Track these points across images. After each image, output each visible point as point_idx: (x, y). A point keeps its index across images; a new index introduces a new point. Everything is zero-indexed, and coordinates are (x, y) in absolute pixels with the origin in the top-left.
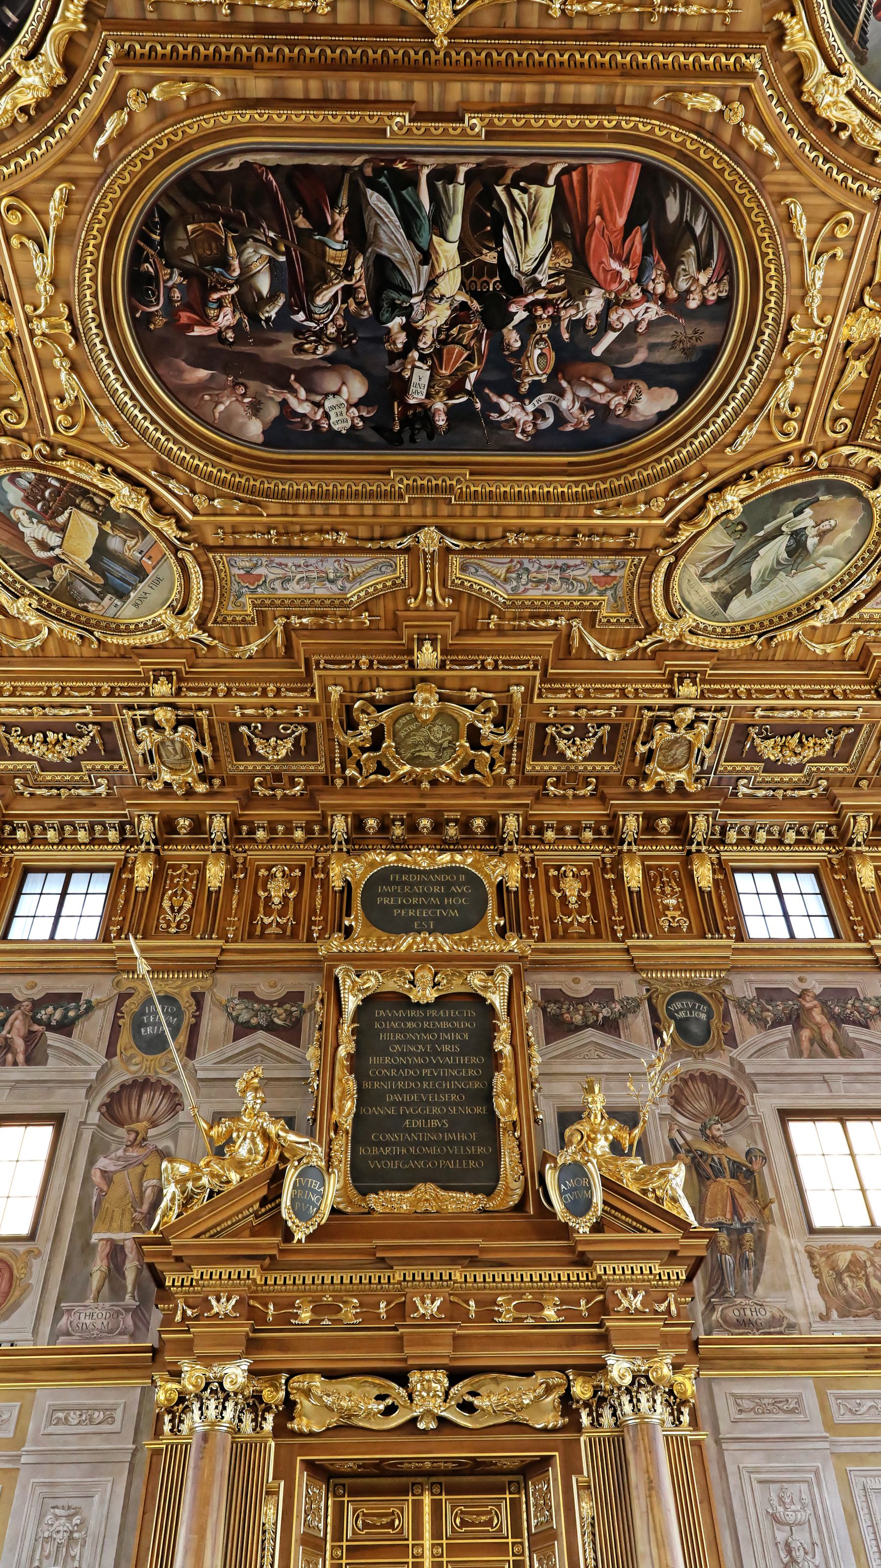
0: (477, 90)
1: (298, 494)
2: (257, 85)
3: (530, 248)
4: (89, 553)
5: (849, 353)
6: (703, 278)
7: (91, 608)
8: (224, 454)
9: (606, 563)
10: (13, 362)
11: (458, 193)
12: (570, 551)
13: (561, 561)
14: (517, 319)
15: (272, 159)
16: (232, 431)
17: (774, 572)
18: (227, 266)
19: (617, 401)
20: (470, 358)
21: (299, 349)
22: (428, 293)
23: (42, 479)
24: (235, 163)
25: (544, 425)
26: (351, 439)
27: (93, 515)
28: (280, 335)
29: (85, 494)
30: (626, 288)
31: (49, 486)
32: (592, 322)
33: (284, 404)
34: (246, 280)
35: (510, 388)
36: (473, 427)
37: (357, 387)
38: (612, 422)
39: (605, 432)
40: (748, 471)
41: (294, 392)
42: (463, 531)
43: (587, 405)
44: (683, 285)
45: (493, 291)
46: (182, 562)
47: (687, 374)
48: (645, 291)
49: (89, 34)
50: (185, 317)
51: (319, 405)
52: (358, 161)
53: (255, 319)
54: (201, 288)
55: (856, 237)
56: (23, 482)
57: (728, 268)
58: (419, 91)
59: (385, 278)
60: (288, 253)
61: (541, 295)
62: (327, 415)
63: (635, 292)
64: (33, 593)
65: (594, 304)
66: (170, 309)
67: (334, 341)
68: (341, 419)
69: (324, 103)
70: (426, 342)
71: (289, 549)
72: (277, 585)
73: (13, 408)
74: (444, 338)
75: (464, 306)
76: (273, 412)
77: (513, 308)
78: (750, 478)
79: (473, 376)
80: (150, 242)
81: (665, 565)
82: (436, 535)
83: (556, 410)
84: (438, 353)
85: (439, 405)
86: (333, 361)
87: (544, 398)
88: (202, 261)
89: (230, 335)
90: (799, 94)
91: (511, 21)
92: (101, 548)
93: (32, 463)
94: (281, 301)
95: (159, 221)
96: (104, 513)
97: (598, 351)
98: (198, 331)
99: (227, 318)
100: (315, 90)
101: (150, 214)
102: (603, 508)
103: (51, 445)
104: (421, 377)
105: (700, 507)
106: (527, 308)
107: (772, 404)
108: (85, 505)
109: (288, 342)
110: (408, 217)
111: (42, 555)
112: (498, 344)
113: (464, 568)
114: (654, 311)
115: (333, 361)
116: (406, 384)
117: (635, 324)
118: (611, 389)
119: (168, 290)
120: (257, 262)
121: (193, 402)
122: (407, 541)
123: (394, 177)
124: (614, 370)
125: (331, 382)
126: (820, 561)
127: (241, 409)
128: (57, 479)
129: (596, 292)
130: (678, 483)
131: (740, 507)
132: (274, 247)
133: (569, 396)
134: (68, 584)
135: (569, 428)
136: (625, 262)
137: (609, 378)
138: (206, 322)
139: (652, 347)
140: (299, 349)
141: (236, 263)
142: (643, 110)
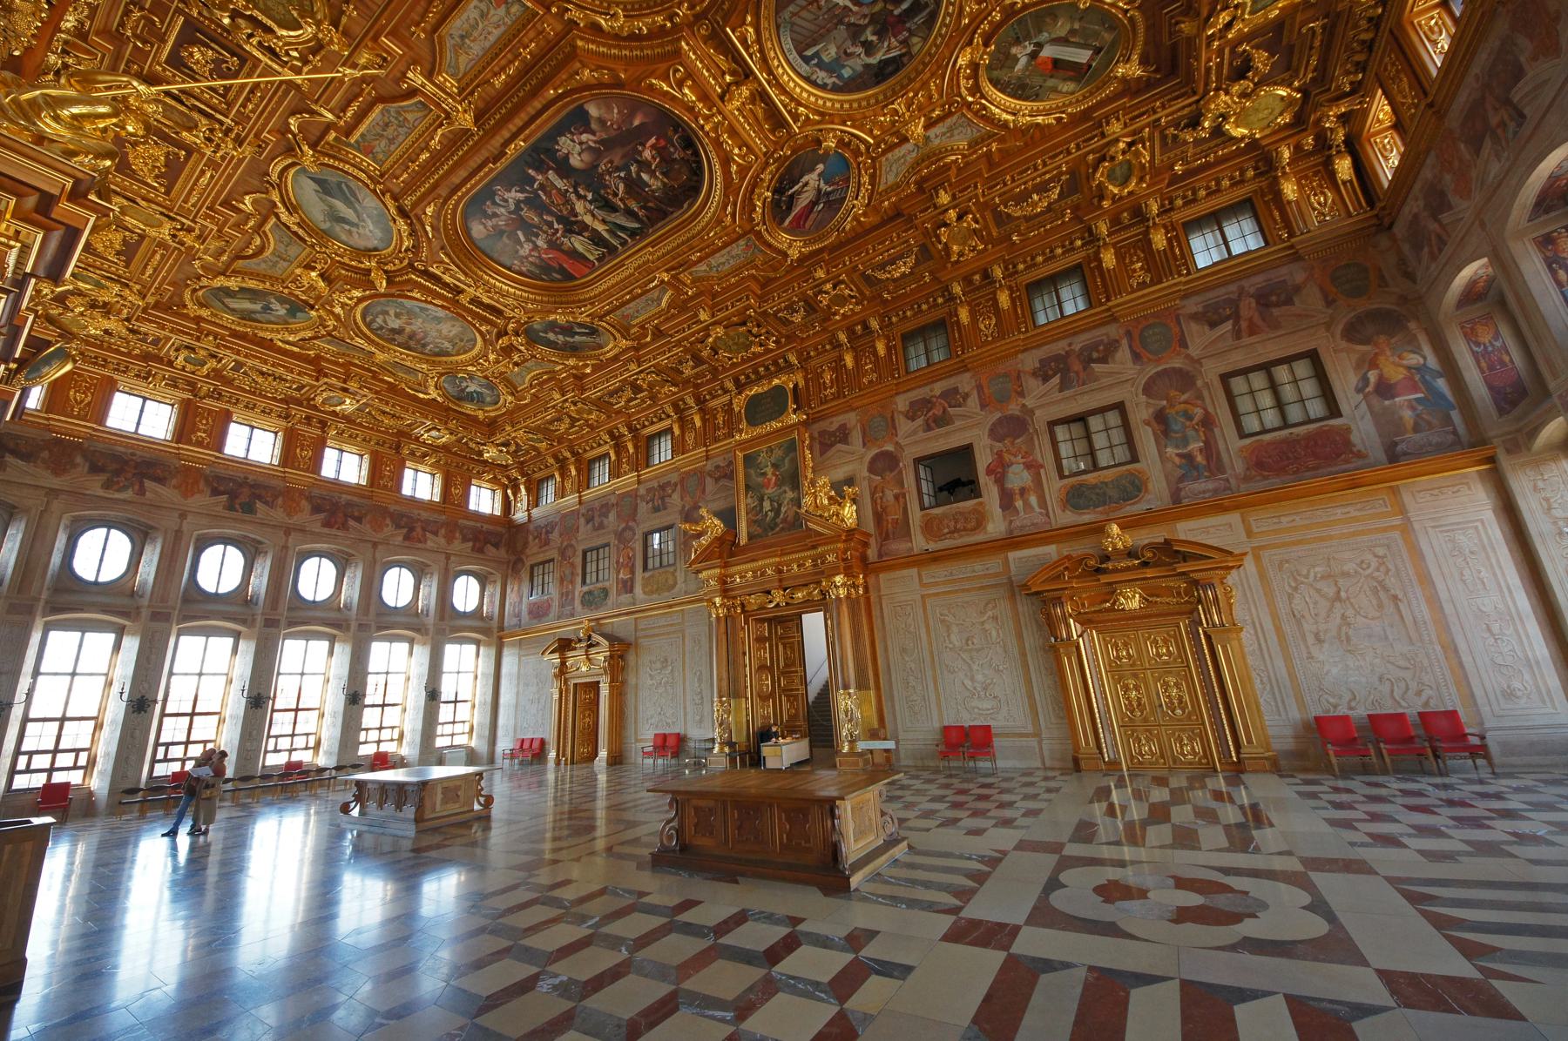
18: (663, 173)
19: (489, 223)
25: (497, 199)
33: (594, 133)
34: (652, 174)
35: (527, 201)
37: (575, 161)
43: (495, 215)
45: (573, 226)
50: (663, 143)
53: (637, 162)
65: (540, 243)
68: (565, 144)
70: (573, 197)
74: (568, 201)
76: (594, 126)
86: (597, 167)
98: (653, 140)
99: (647, 154)
104: (560, 184)
110: (623, 228)
112: (551, 213)
120: (654, 182)
125: (586, 157)
138: (653, 147)
140: (611, 162)
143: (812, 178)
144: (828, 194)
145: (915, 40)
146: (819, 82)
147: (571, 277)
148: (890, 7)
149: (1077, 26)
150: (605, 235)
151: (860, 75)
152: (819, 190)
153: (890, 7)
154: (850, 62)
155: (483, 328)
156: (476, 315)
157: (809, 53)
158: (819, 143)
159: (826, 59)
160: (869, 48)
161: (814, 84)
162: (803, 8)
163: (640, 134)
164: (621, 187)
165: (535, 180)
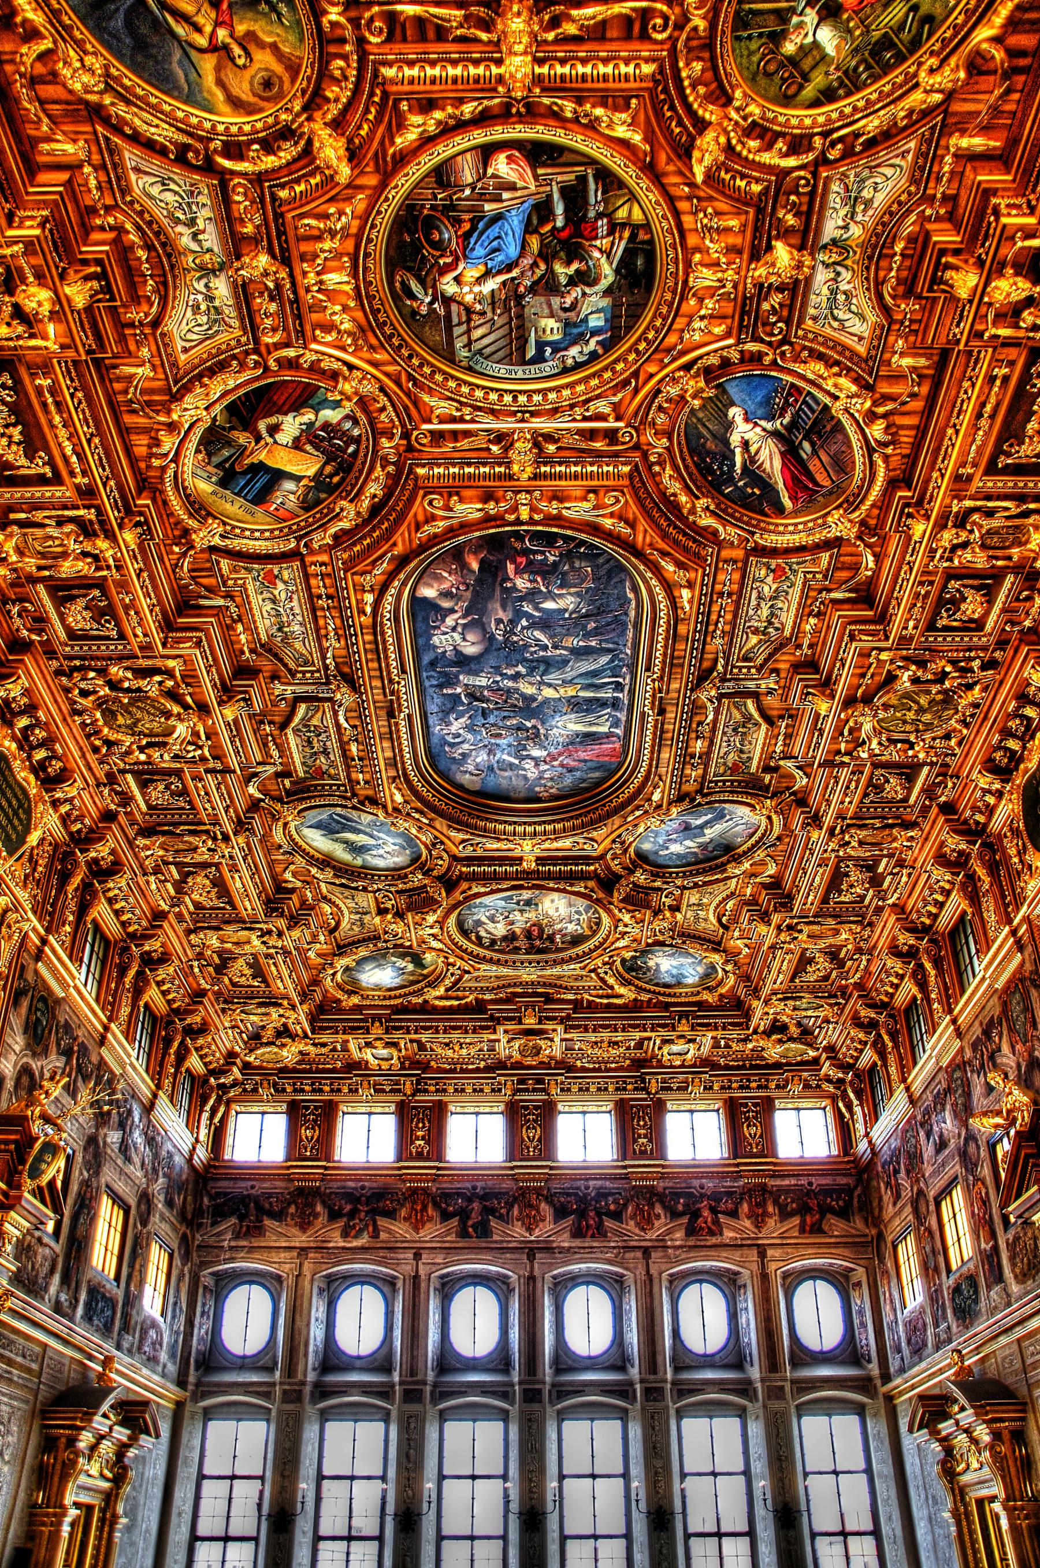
7: (200, 457)
11: (607, 694)
16: (425, 579)
17: (346, 842)
18: (561, 587)
22: (542, 683)
25: (449, 739)
27: (320, 472)
31: (348, 446)
33: (452, 611)
34: (550, 596)
37: (470, 650)
56: (348, 425)
66: (526, 552)
68: (443, 640)
76: (446, 604)
88: (564, 574)
92: (278, 476)
98: (510, 568)
104: (482, 681)
106: (534, 727)
108: (328, 469)
110: (595, 674)
111: (262, 426)
120: (565, 602)
127: (445, 586)
128: (356, 452)
132: (574, 612)
134: (229, 443)
138: (518, 572)
140: (499, 621)
143: (742, 431)
144: (793, 426)
145: (622, 214)
146: (581, 359)
148: (548, 228)
151: (616, 306)
152: (775, 434)
153: (548, 228)
154: (585, 310)
156: (559, 877)
157: (531, 352)
159: (556, 337)
160: (584, 278)
161: (578, 366)
162: (468, 332)
163: (492, 572)
164: (538, 634)
165: (459, 696)
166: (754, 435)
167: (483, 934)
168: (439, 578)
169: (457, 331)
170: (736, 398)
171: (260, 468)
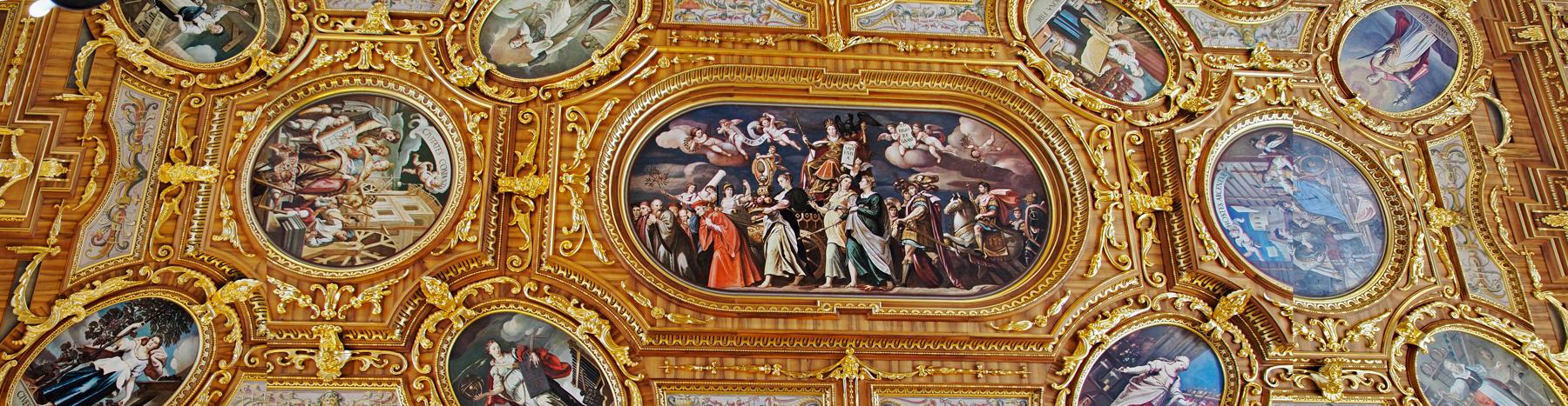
0: (828, 326)
1: (939, 79)
2: (967, 329)
3: (778, 239)
4: (1089, 42)
5: (535, 168)
6: (653, 219)
8: (990, 110)
9: (691, 19)
10: (1129, 174)
11: (830, 271)
12: (722, 30)
13: (727, 22)
14: (783, 194)
15: (952, 291)
18: (983, 231)
19: (701, 139)
20: (813, 171)
21: (935, 179)
23: (1118, 97)
24: (975, 289)
25: (754, 124)
26: (896, 118)
27: (1085, 70)
28: (947, 188)
29: (1089, 85)
30: (707, 214)
32: (728, 192)
33: (945, 144)
34: (970, 223)
36: (809, 125)
37: (893, 154)
38: (704, 126)
39: (708, 118)
40: (592, 87)
41: (938, 152)
42: (807, 48)
43: (724, 137)
44: (666, 214)
45: (800, 210)
46: (1024, 31)
47: (651, 156)
48: (693, 211)
49: (1061, 356)
50: (1012, 201)
51: (920, 142)
52: (896, 290)
53: (965, 198)
54: (1000, 220)
55: (555, 241)
56: (1132, 95)
57: (637, 225)
58: (865, 326)
59: (877, 223)
60: (942, 238)
61: (767, 210)
62: (914, 135)
63: (700, 211)
64: (1135, 13)
66: (1021, 205)
67: (910, 184)
68: (903, 132)
69: (925, 320)
70: (846, 182)
71: (941, 39)
72: (949, 12)
73: (1133, 145)
74: (833, 183)
75: (821, 204)
76: (952, 138)
77: (786, 202)
78: (590, 81)
79: (810, 158)
80: (1032, 246)
81: (645, 16)
82: (830, 45)
83: (747, 135)
84: (836, 174)
85: (833, 138)
86: (911, 171)
87: (757, 143)
89: (982, 189)
90: (611, 323)
91: (804, 362)
92: (1081, 45)
93: (1125, 108)
94: (946, 210)
95: (1025, 258)
96: (1078, 70)
97: (721, 174)
98: (1003, 192)
99: (983, 200)
100: (931, 326)
101: (1030, 261)
102: (707, 61)
103: (1109, 118)
105: (626, 60)
106: (776, 202)
107: (591, 135)
108: (1089, 77)
109: (943, 183)
110: (862, 257)
112: (794, 179)
113: (804, 19)
114: (684, 198)
115: (910, 171)
116: (859, 154)
117: (696, 191)
118: (707, 148)
119: (1022, 217)
120: (962, 233)
121: (1008, 146)
122: (852, 42)
123: (871, 279)
124: (707, 160)
125: (912, 158)
126: (514, 15)
127: (976, 141)
129: (729, 212)
130: (650, 80)
131: (594, 58)
132: (951, 242)
133: (738, 144)
135: (735, 121)
136: (710, 229)
137: (710, 155)
139: (682, 175)
140: (935, 179)
141: (977, 232)
142: (719, 315)
143: (1167, 369)
147: (702, 280)
149: (1517, 380)
150: (830, 252)
152: (1168, 396)
155: (464, 228)
158: (1206, 320)
166: (1164, 378)
167: (329, 121)
168: (984, 137)
169: (1247, 164)
170: (1195, 361)
171: (1086, 33)
